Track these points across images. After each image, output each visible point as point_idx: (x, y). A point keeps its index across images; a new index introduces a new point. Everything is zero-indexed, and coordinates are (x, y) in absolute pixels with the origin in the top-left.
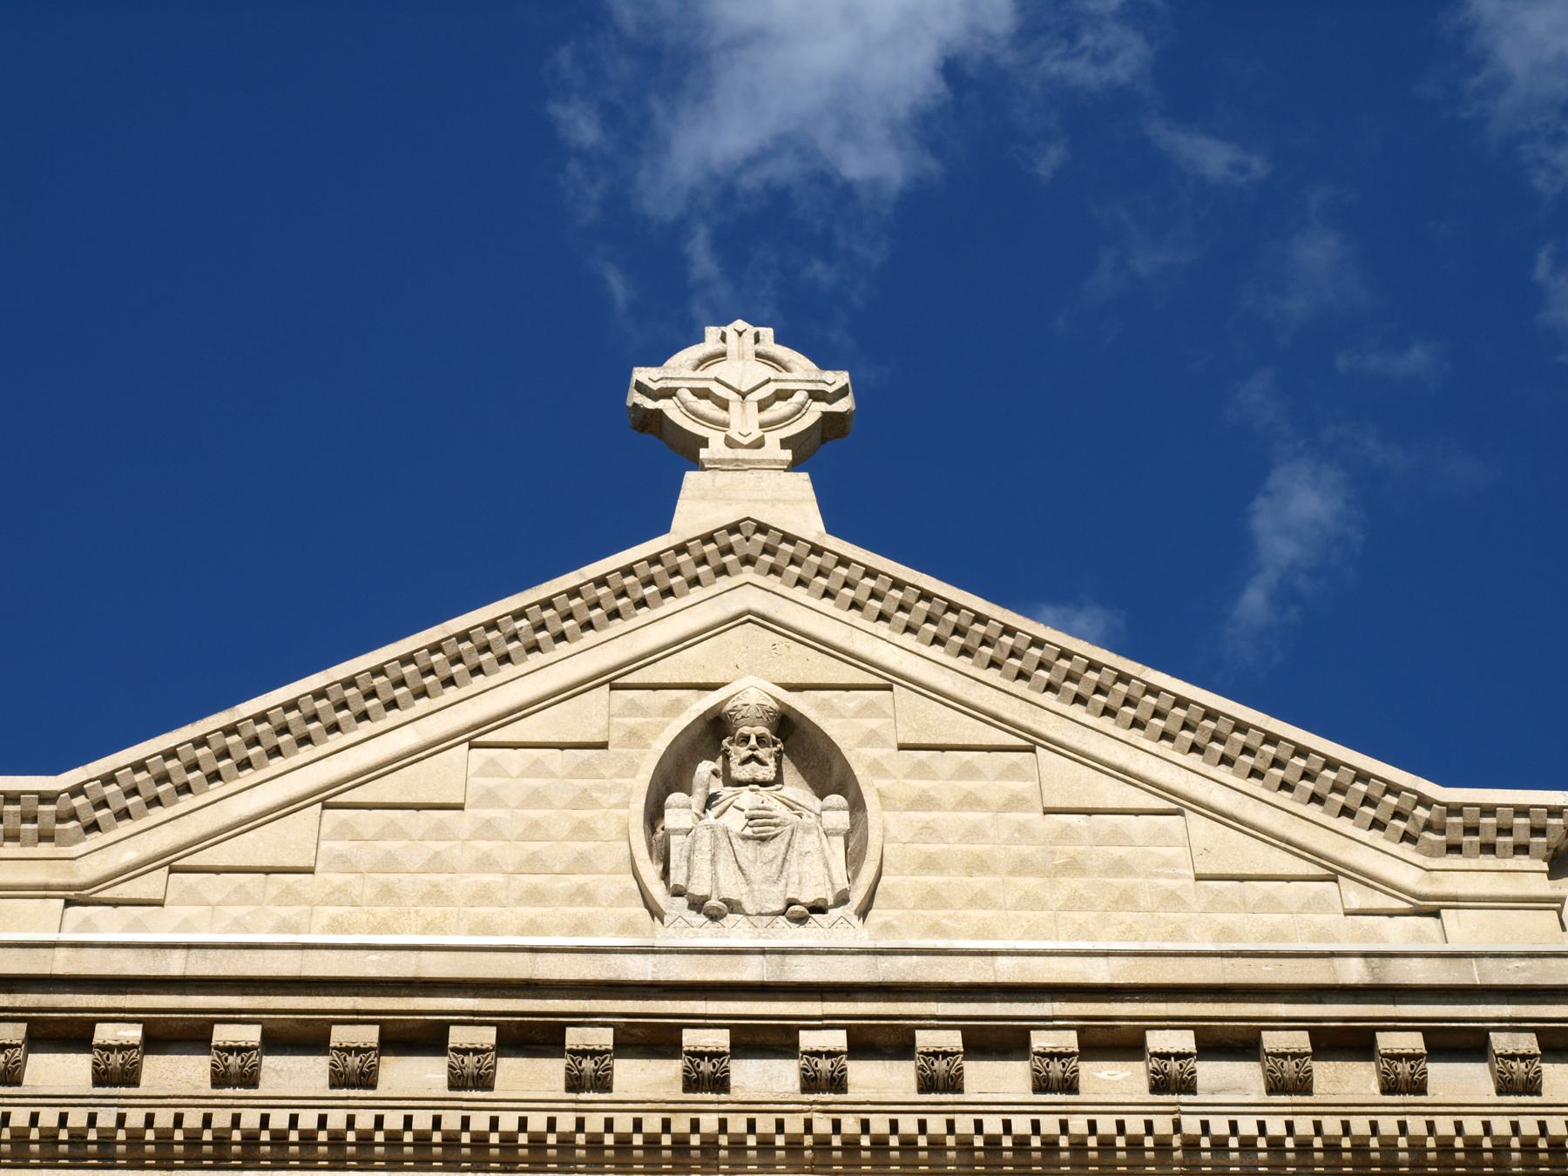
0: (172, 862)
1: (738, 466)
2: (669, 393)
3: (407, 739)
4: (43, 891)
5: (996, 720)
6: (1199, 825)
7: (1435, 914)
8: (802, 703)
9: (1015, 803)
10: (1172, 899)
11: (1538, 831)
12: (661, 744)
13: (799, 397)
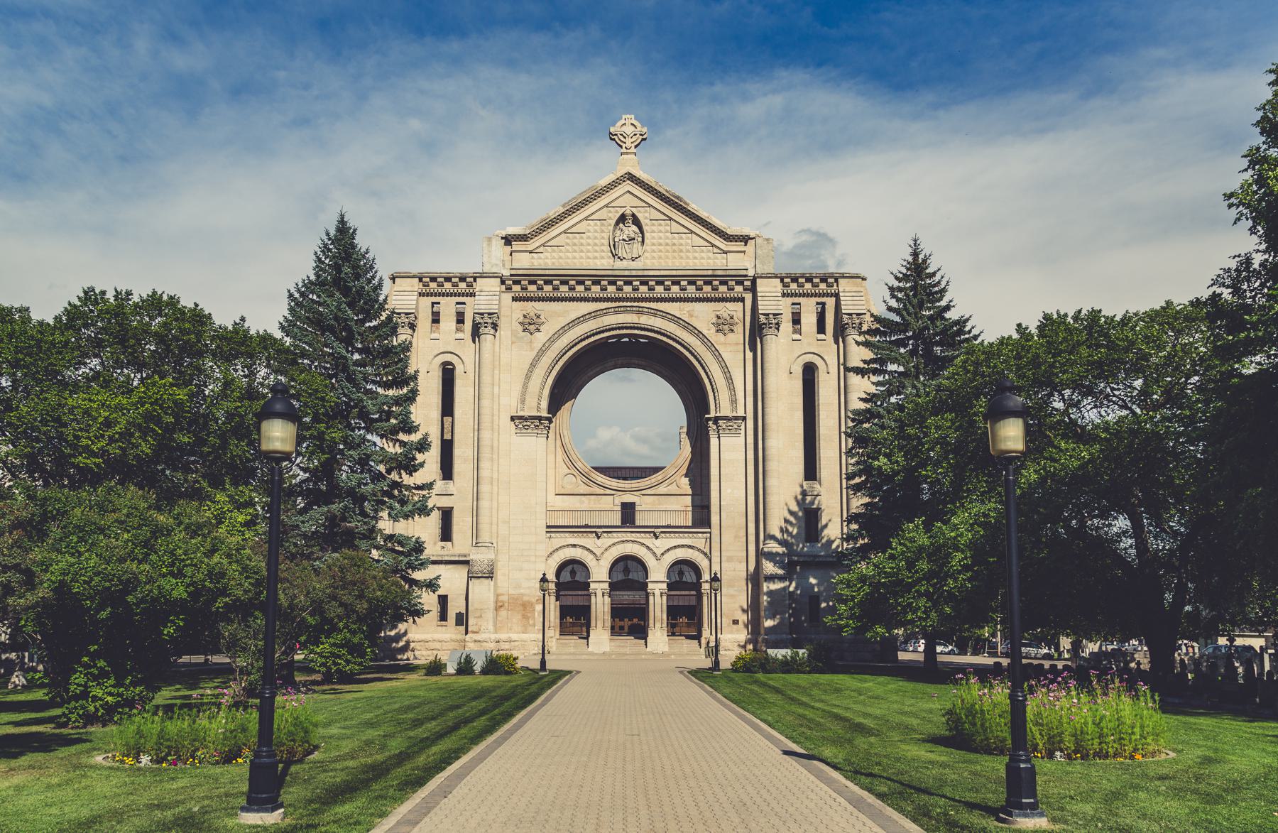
1: (627, 153)
2: (616, 135)
5: (665, 215)
9: (667, 232)
10: (688, 251)
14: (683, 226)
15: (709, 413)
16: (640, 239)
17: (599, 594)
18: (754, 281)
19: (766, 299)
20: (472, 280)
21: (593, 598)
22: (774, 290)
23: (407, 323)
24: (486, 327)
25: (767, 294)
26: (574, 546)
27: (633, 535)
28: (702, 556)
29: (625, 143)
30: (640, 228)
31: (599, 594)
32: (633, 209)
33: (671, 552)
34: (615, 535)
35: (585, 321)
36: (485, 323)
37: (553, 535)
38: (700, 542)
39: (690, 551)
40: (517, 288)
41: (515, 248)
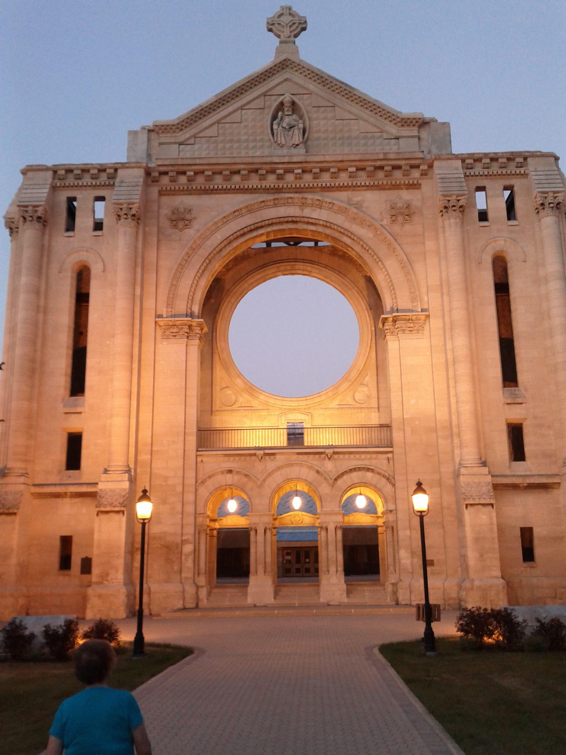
0: (195, 136)
3: (230, 109)
4: (175, 143)
6: (361, 122)
7: (398, 139)
8: (296, 99)
11: (417, 122)
12: (271, 114)
13: (297, 25)
14: (350, 112)
15: (383, 314)
16: (301, 126)
17: (261, 531)
18: (431, 166)
19: (447, 180)
20: (112, 171)
21: (252, 533)
22: (455, 172)
23: (35, 218)
24: (126, 219)
25: (448, 176)
26: (230, 471)
27: (301, 456)
28: (384, 481)
29: (283, 32)
30: (301, 117)
31: (261, 531)
32: (293, 97)
33: (345, 477)
34: (278, 457)
35: (242, 215)
36: (126, 214)
37: (205, 459)
38: (380, 462)
39: (369, 475)
40: (165, 180)
41: (163, 140)
